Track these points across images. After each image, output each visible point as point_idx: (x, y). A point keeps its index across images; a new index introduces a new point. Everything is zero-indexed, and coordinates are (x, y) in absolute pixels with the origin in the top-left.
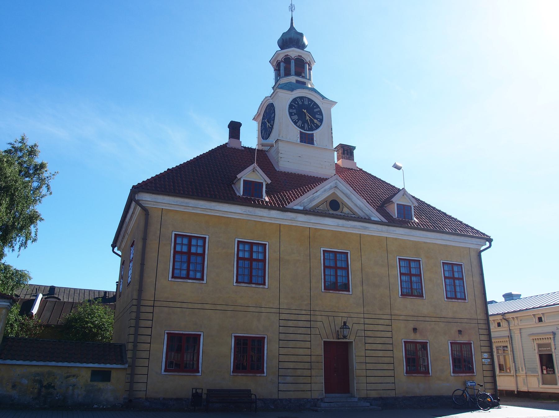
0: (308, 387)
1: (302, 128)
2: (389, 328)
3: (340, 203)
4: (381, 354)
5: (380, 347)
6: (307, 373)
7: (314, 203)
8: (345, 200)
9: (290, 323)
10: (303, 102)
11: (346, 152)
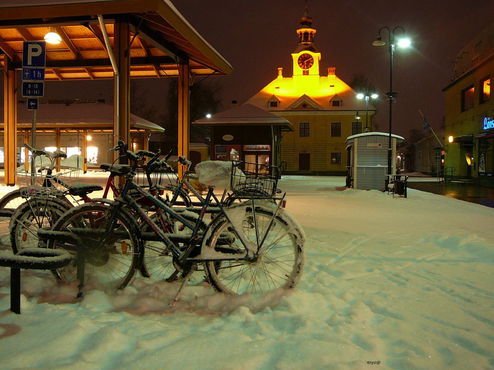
0: (293, 168)
1: (304, 68)
2: (325, 148)
3: (307, 105)
4: (321, 157)
5: (320, 155)
6: (293, 163)
7: (295, 107)
8: (309, 103)
9: (287, 148)
10: (304, 56)
11: (331, 71)
